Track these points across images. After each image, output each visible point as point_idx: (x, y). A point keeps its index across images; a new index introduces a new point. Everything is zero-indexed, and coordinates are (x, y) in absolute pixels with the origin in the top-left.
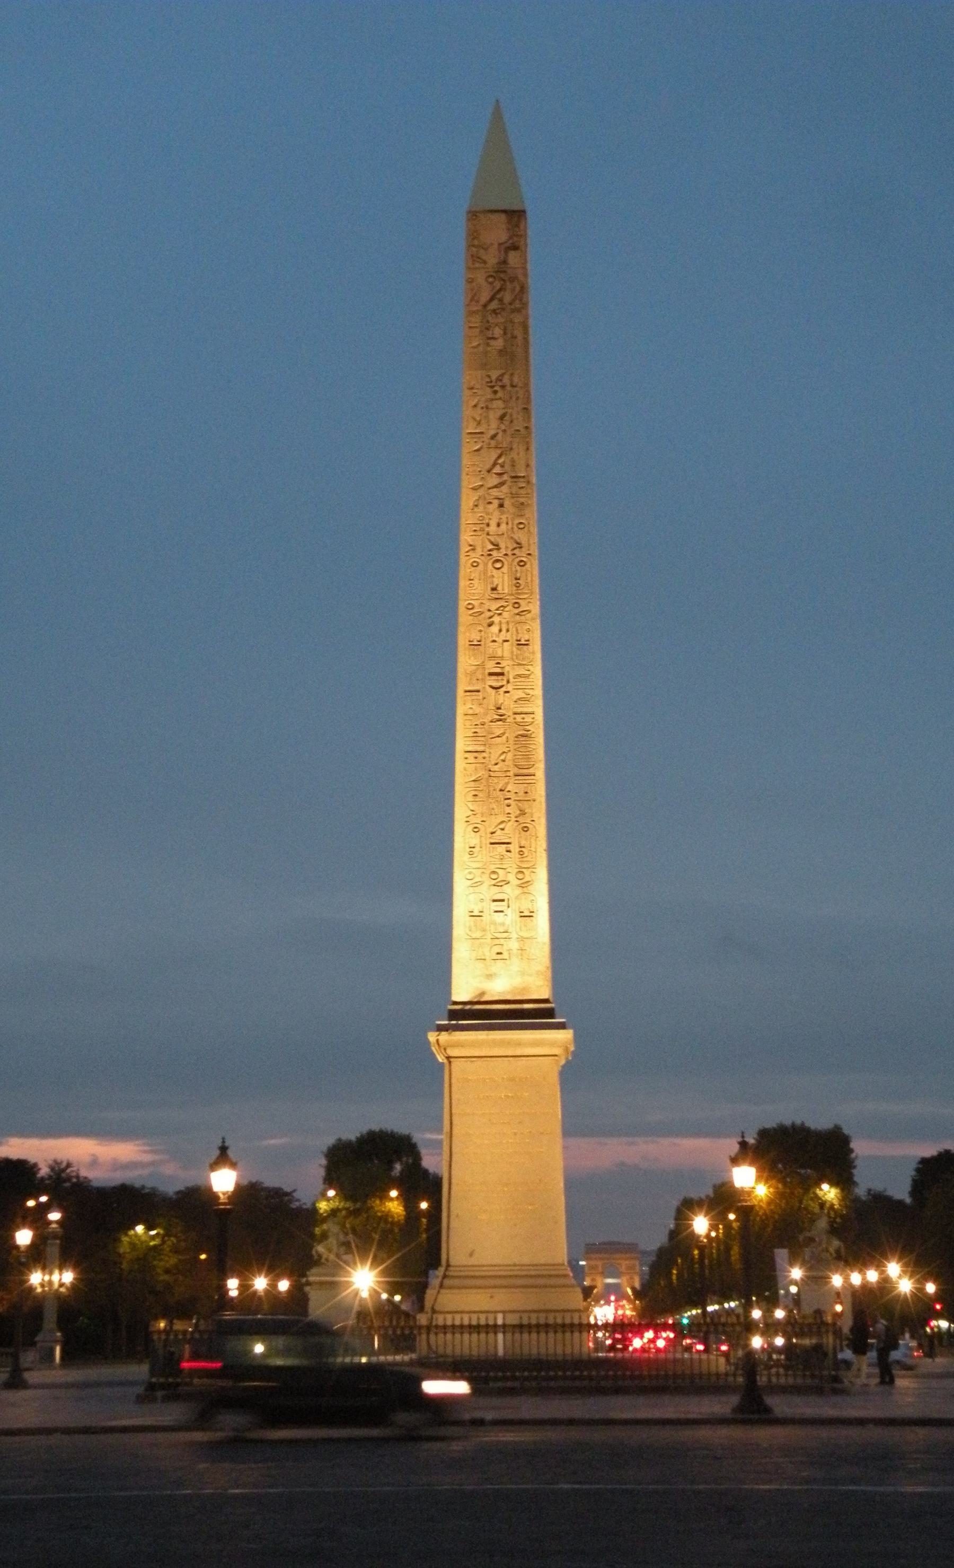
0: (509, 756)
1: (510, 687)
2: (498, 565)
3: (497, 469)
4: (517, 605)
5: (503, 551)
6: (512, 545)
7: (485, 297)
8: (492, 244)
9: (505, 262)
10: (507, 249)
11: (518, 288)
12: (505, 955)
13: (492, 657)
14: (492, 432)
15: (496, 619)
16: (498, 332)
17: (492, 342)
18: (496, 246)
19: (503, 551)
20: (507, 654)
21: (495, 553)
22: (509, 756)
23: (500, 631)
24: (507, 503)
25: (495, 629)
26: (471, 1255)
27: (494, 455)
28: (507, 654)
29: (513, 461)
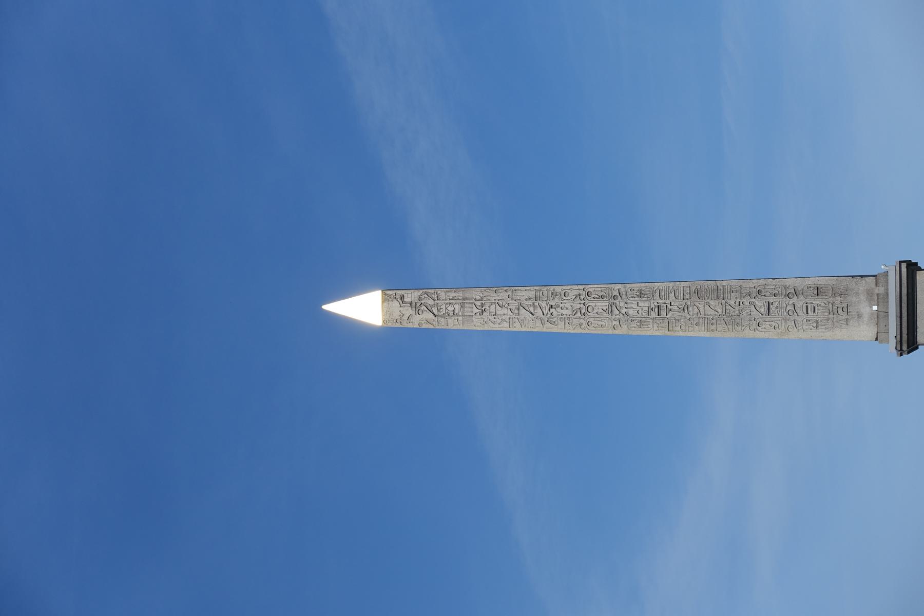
0: (712, 303)
1: (668, 302)
3: (532, 309)
4: (615, 297)
9: (411, 304)
15: (624, 311)
16: (450, 308)
17: (456, 311)
19: (582, 306)
21: (583, 311)
22: (712, 303)
24: (553, 304)
25: (631, 312)
27: (523, 311)
29: (526, 300)
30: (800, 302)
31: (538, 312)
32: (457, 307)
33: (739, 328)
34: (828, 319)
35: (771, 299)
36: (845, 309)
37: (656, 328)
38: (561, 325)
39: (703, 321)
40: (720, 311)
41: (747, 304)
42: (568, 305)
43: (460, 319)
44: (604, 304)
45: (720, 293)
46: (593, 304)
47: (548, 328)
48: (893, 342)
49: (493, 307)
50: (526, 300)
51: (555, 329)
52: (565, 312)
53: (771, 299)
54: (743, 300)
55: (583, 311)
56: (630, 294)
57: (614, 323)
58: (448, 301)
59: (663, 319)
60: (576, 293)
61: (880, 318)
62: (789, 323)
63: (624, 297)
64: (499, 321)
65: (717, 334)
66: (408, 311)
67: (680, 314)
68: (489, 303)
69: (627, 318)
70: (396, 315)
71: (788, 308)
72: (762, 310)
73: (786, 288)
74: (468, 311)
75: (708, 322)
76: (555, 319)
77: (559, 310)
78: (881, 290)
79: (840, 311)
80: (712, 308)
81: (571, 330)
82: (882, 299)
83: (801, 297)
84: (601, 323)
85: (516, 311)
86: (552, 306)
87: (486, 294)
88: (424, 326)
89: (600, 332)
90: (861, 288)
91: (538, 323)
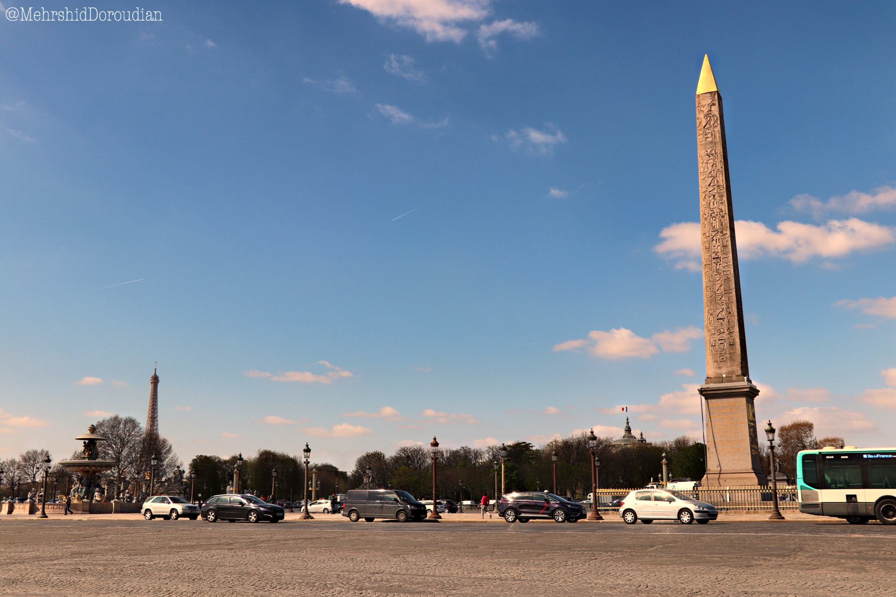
4: (722, 232)
16: (709, 135)
30: (725, 336)
35: (726, 320)
38: (704, 203)
44: (718, 226)
47: (702, 196)
48: (706, 386)
51: (701, 200)
53: (726, 320)
56: (725, 241)
61: (720, 379)
65: (704, 292)
66: (706, 110)
78: (734, 378)
81: (702, 209)
82: (729, 379)
91: (704, 189)
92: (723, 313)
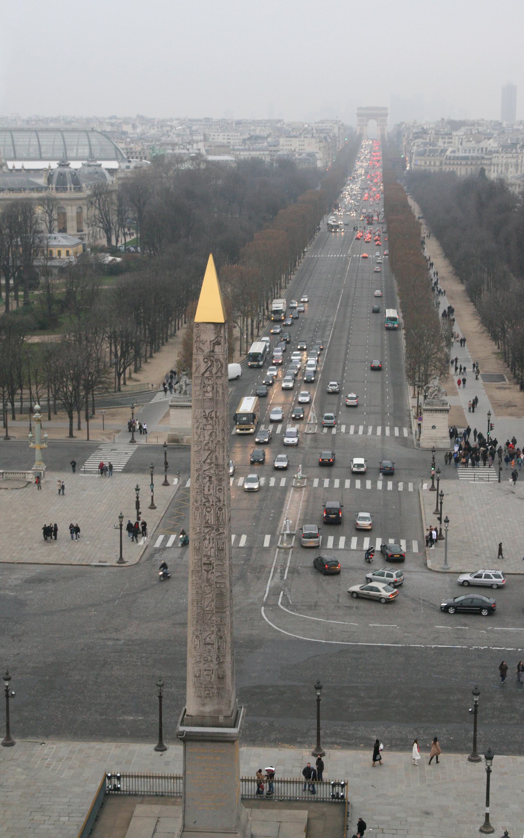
1: (214, 570)
2: (208, 509)
3: (208, 461)
4: (218, 530)
5: (211, 503)
6: (215, 500)
7: (202, 370)
8: (206, 341)
9: (213, 351)
10: (214, 344)
11: (220, 366)
12: (211, 695)
13: (206, 556)
14: (207, 441)
15: (208, 537)
16: (209, 388)
17: (207, 394)
18: (208, 342)
19: (211, 503)
20: (212, 554)
21: (207, 504)
22: (213, 604)
23: (209, 543)
24: (213, 479)
25: (207, 542)
26: (195, 822)
28: (212, 554)
29: (216, 457)
30: (214, 666)
31: (206, 467)
32: (210, 395)
33: (195, 622)
34: (201, 684)
35: (216, 646)
36: (208, 696)
37: (194, 561)
39: (201, 595)
40: (207, 609)
41: (212, 629)
42: (211, 490)
43: (201, 397)
44: (212, 520)
45: (220, 609)
46: (212, 512)
49: (210, 427)
50: (216, 457)
52: (206, 489)
54: (215, 627)
55: (207, 504)
56: (220, 542)
57: (198, 529)
58: (215, 386)
59: (201, 567)
60: (221, 498)
62: (198, 657)
63: (218, 537)
64: (199, 432)
66: (207, 349)
67: (205, 580)
68: (214, 423)
69: (202, 539)
70: (204, 337)
71: (209, 658)
72: (208, 639)
73: (224, 656)
74: (207, 404)
75: (199, 602)
76: (200, 480)
77: (208, 484)
79: (207, 692)
80: (210, 604)
83: (217, 667)
84: (198, 518)
85: (206, 448)
86: (210, 477)
87: (221, 421)
88: (194, 364)
89: (191, 517)
90: (223, 707)
91: (198, 466)
92: (213, 637)
